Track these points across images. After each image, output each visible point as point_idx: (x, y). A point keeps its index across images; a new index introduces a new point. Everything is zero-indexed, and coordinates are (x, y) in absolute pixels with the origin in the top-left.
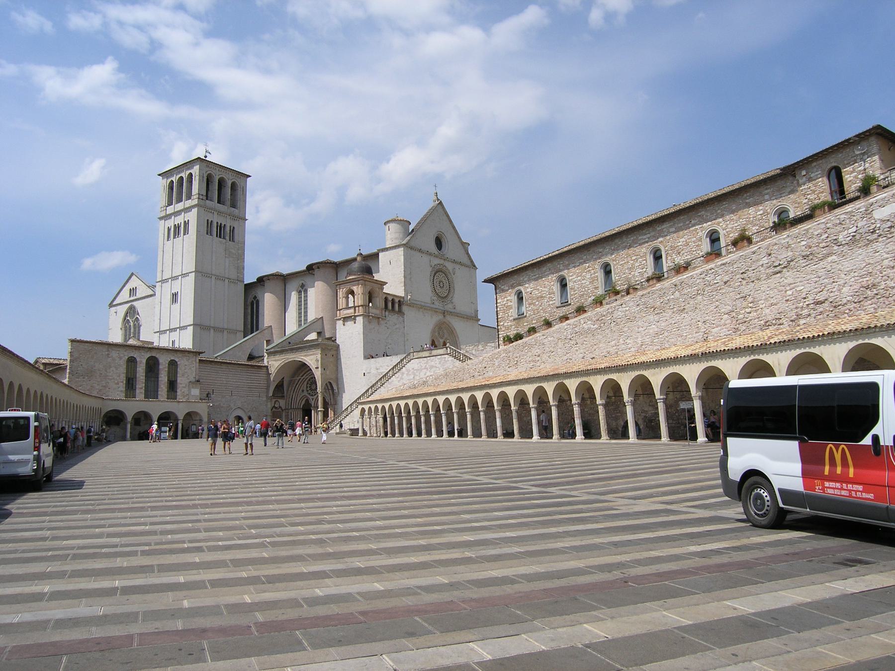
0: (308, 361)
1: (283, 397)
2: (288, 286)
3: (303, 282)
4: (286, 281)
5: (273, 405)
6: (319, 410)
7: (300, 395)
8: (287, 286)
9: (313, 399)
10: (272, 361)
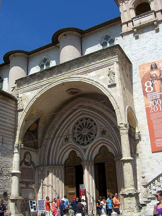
0: (92, 78)
1: (36, 147)
2: (31, 63)
3: (46, 57)
4: (29, 60)
5: (23, 158)
6: (123, 158)
7: (63, 145)
9: (85, 150)
10: (24, 92)
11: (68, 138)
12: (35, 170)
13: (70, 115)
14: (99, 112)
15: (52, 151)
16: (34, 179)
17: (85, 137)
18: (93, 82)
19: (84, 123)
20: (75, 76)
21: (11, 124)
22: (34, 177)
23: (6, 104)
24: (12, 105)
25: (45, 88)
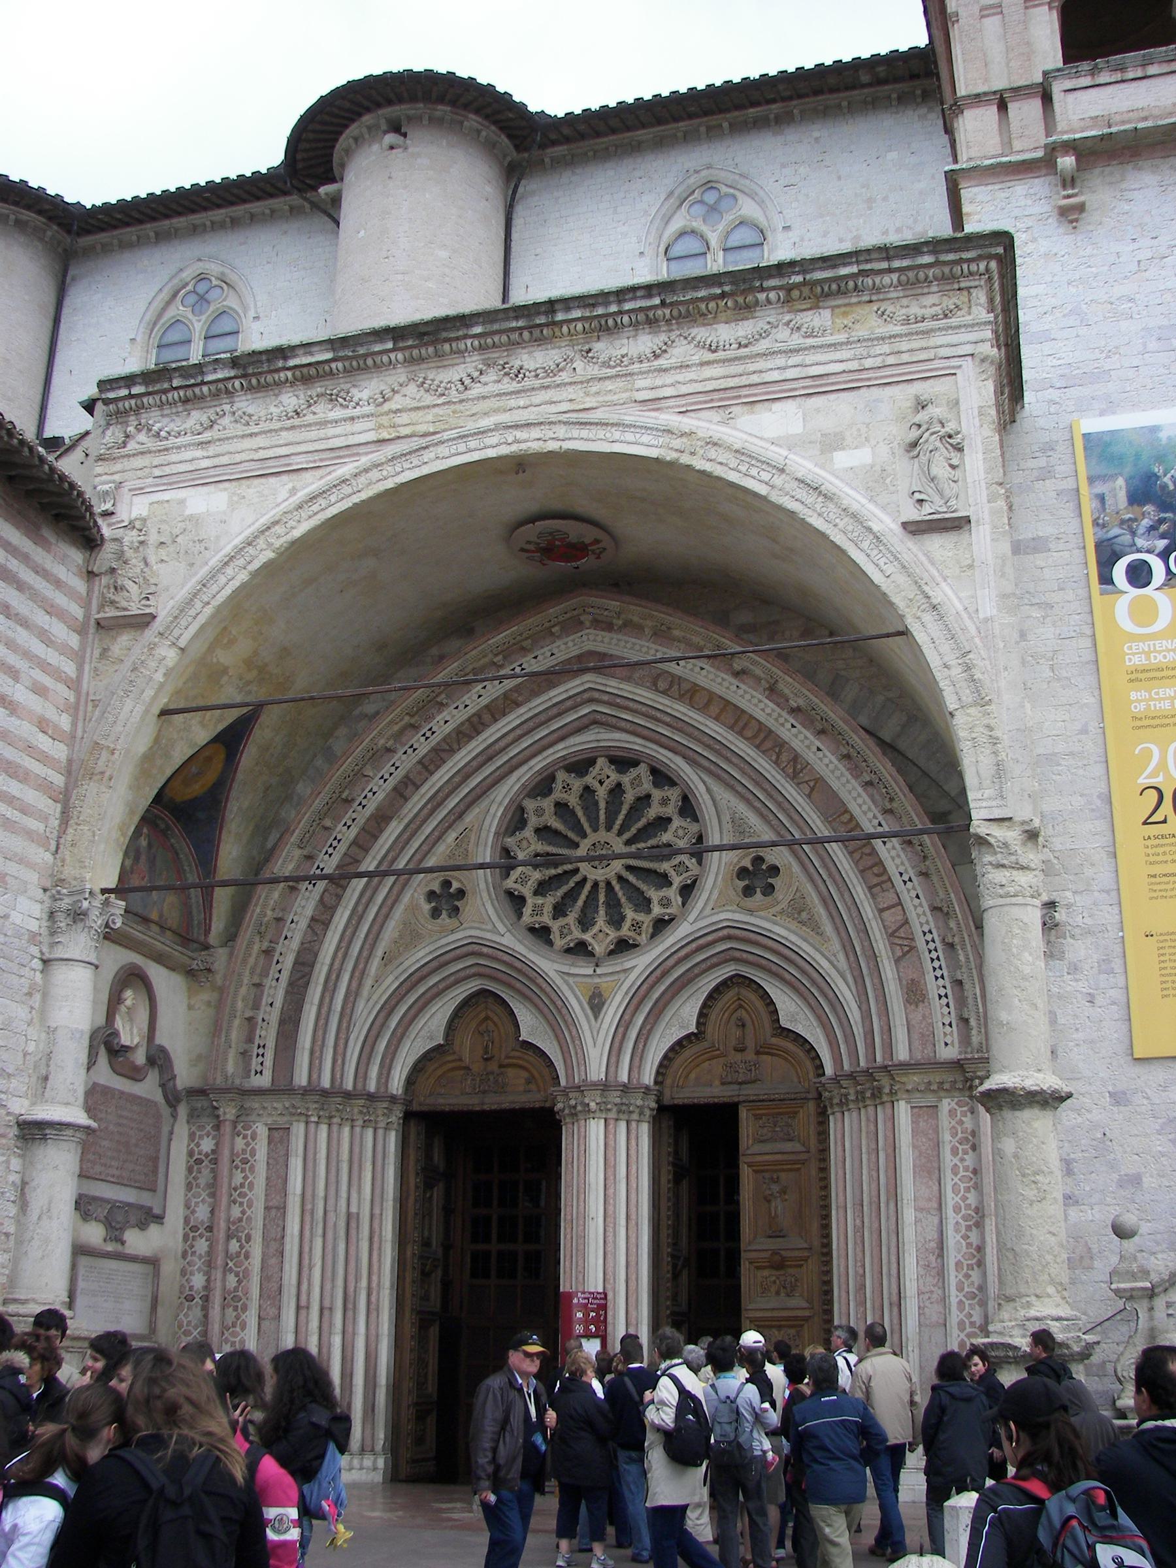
0: (777, 454)
3: (214, 268)
4: (71, 273)
7: (410, 937)
8: (77, 297)
9: (596, 1003)
11: (461, 893)
12: (174, 1116)
13: (496, 720)
14: (740, 721)
15: (322, 979)
16: (161, 1187)
17: (602, 898)
18: (778, 480)
19: (602, 793)
20: (632, 415)
21: (43, 725)
22: (162, 1170)
23: (25, 558)
24: (61, 572)
25: (366, 470)
